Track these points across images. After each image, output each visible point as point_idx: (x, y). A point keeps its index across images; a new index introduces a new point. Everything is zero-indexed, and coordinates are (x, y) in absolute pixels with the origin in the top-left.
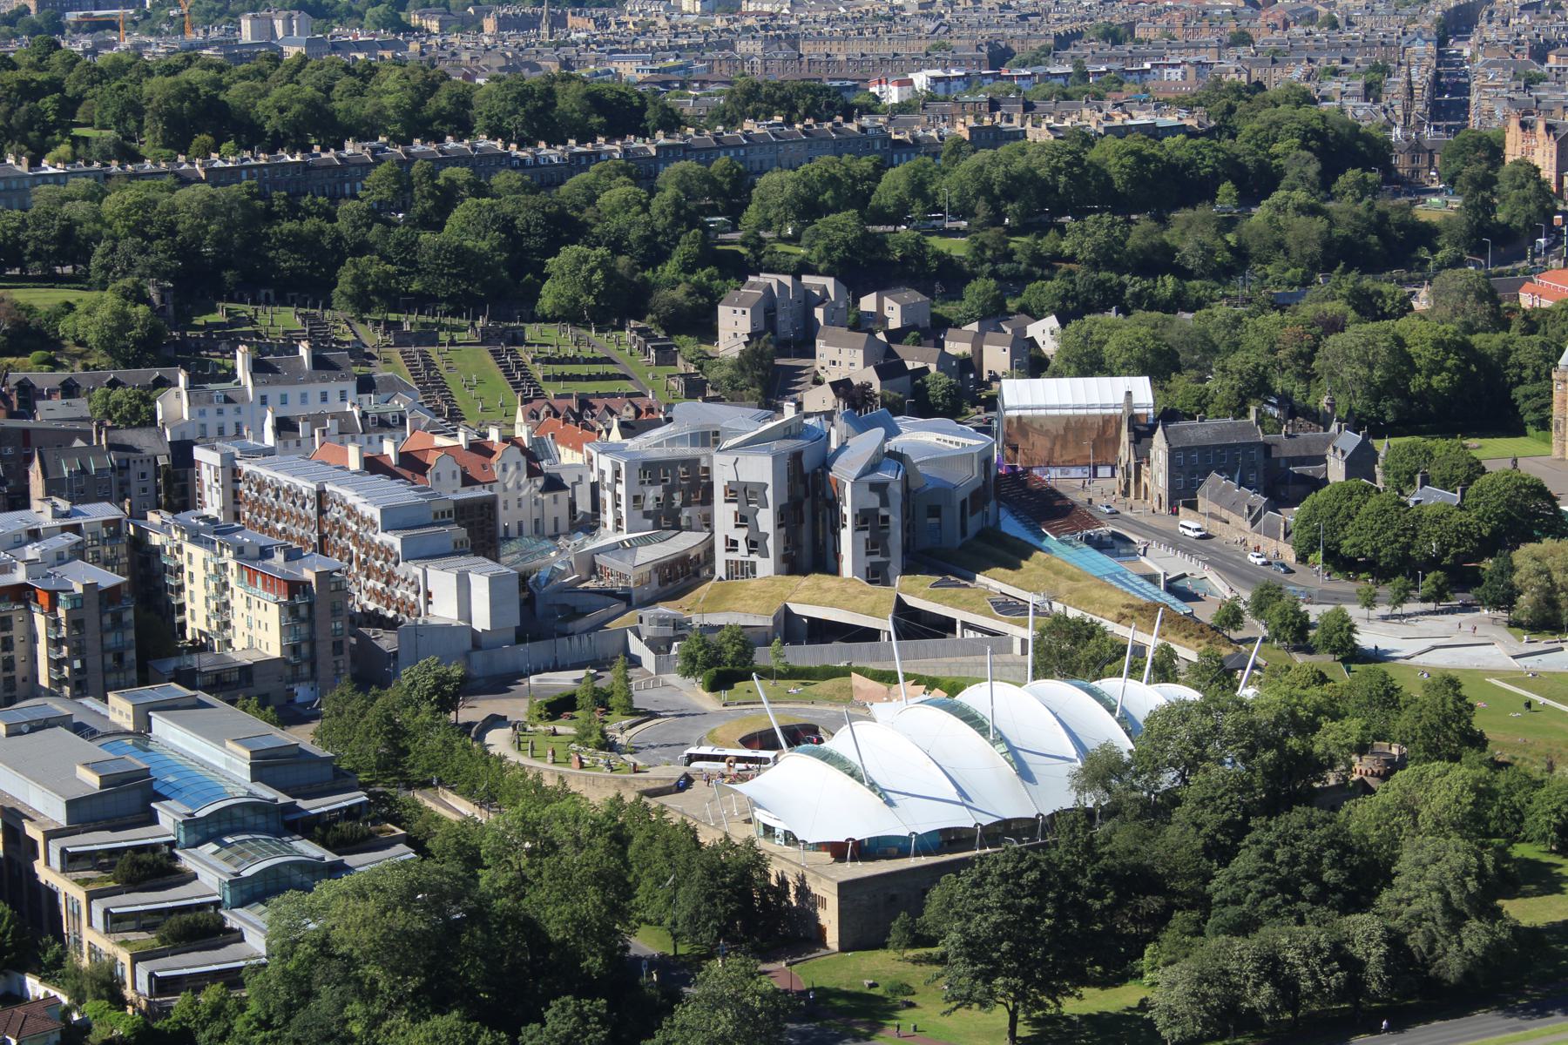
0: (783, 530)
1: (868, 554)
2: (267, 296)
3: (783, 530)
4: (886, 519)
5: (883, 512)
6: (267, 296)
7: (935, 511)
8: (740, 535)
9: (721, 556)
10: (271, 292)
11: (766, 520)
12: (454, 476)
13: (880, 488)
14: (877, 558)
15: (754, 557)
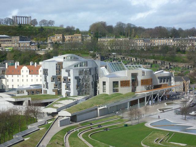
0: (54, 83)
1: (66, 89)
2: (134, 59)
3: (54, 83)
4: (70, 80)
5: (69, 78)
6: (134, 59)
7: (104, 83)
8: (45, 83)
9: (43, 89)
10: (135, 59)
11: (49, 79)
12: (27, 72)
13: (68, 71)
14: (67, 91)
15: (46, 89)
